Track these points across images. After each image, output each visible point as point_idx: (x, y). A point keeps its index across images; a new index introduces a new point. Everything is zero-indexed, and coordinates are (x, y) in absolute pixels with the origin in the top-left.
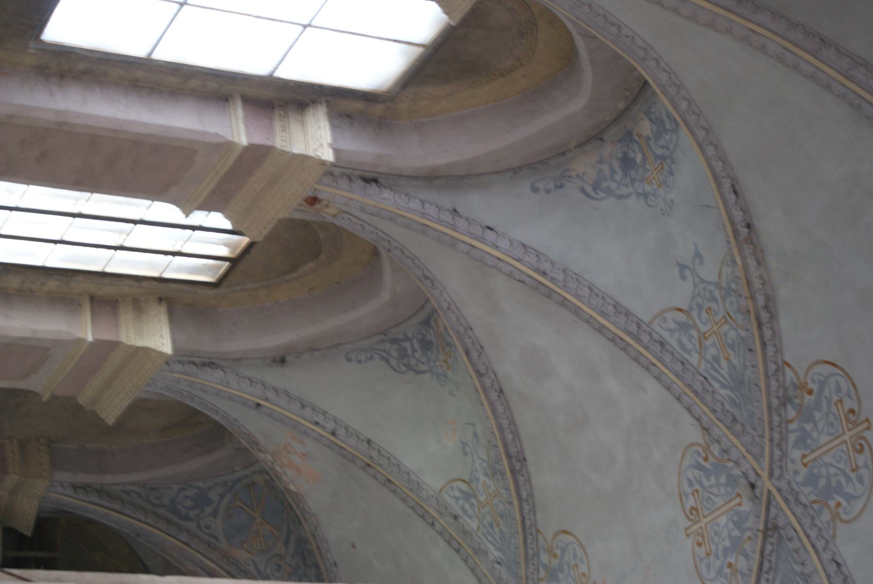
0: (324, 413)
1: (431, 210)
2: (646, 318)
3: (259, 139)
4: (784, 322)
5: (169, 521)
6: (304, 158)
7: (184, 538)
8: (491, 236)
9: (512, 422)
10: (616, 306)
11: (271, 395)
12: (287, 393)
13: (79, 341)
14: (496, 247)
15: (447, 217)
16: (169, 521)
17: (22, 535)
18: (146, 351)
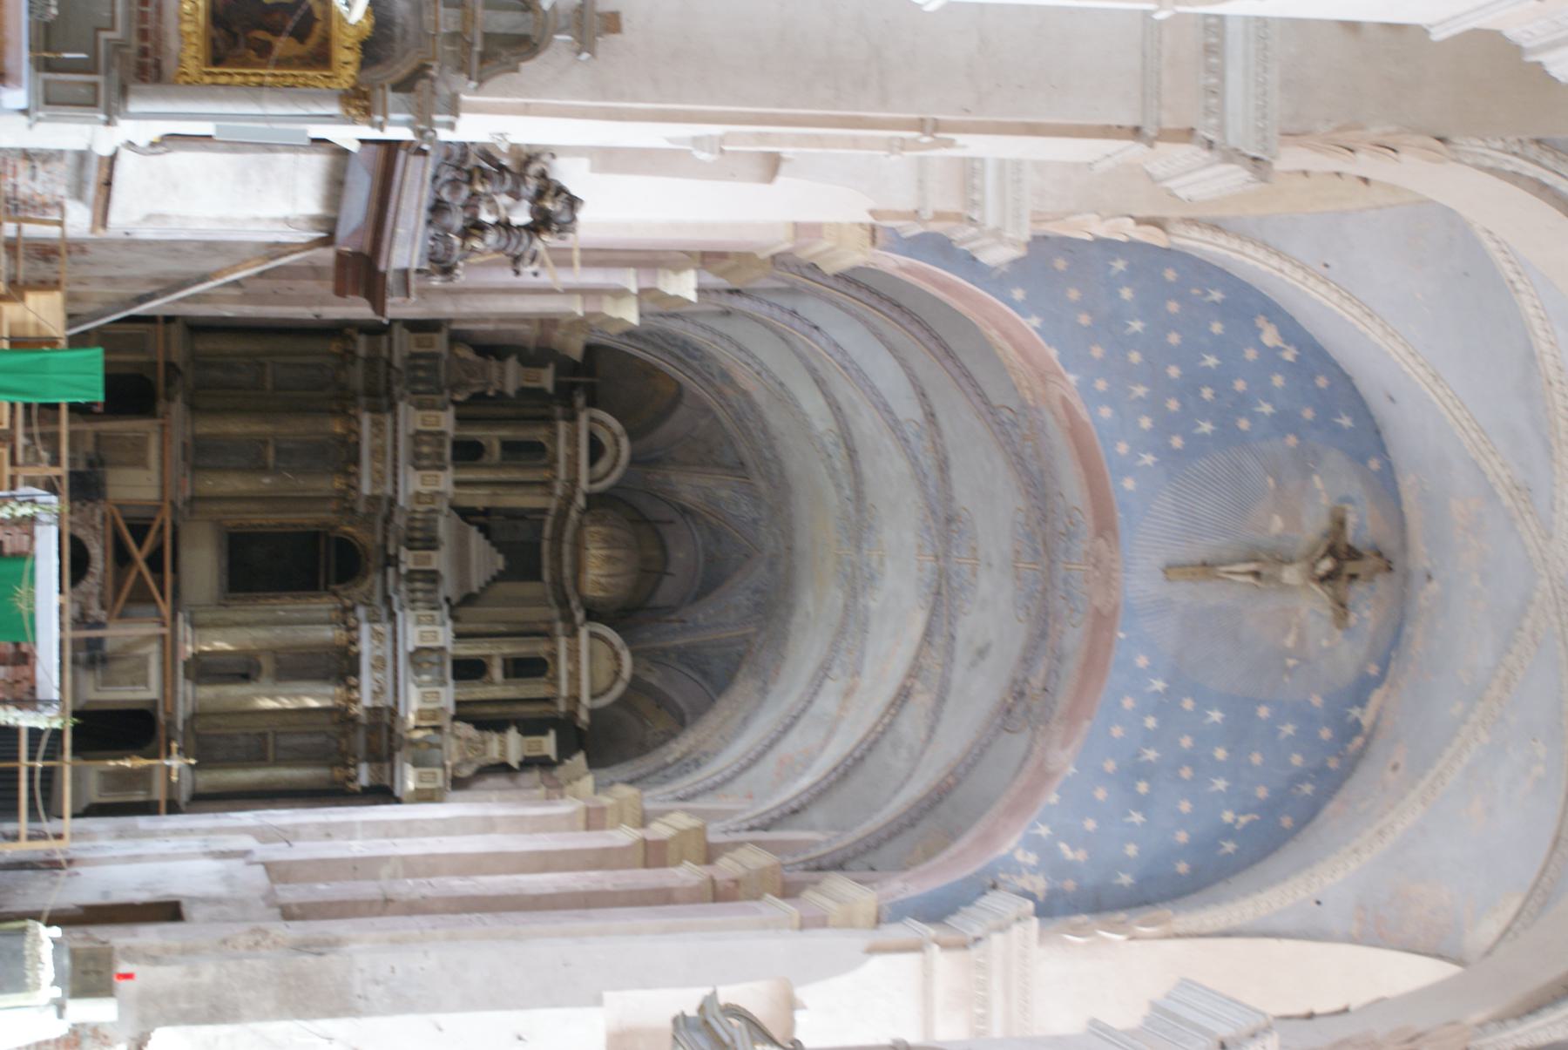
0: (753, 357)
1: (776, 312)
2: (900, 418)
3: (646, 284)
4: (954, 474)
5: (678, 358)
6: (677, 297)
7: (690, 373)
8: (815, 334)
9: (848, 429)
10: (886, 405)
11: (717, 339)
12: (729, 339)
13: (574, 313)
14: (817, 343)
15: (787, 318)
16: (678, 358)
17: (575, 362)
18: (621, 320)
